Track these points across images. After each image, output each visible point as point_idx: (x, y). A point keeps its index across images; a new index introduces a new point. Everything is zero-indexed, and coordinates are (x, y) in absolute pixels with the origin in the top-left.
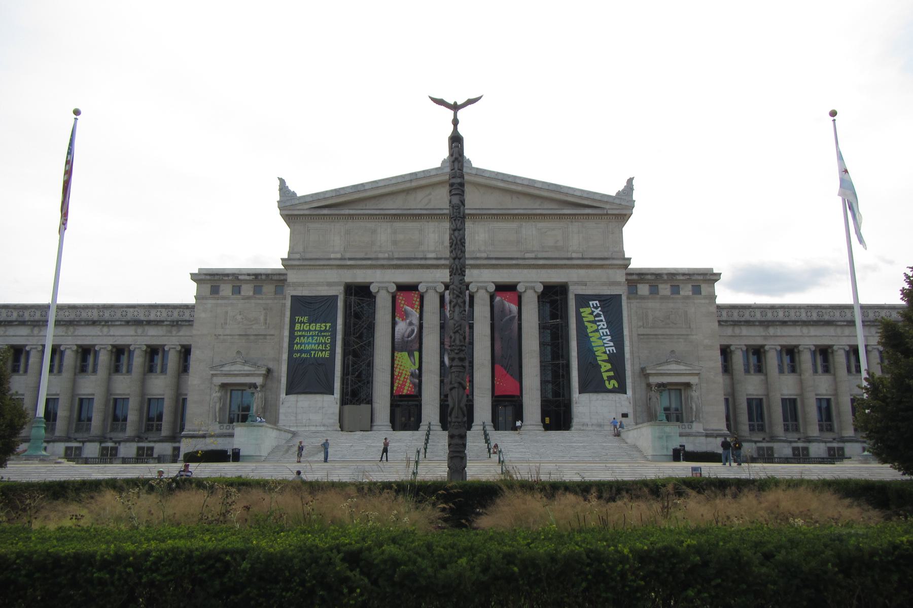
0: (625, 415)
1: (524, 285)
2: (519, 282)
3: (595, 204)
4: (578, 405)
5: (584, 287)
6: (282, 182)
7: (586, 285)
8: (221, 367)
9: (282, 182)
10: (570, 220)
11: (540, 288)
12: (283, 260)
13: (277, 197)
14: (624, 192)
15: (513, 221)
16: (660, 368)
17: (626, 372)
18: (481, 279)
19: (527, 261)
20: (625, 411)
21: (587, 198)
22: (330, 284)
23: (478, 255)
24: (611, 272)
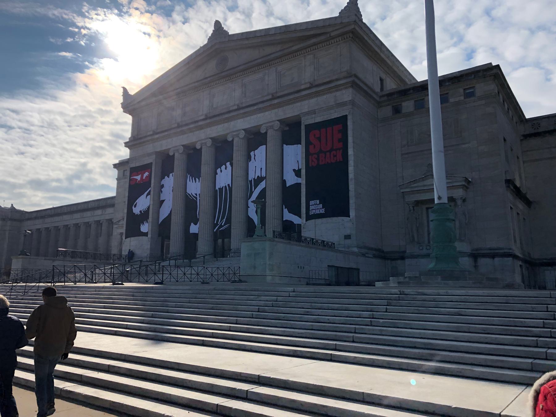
0: (348, 237)
1: (265, 126)
2: (262, 125)
3: (319, 32)
4: (305, 230)
5: (314, 115)
6: (124, 89)
7: (315, 114)
8: (119, 222)
9: (124, 89)
10: (303, 55)
11: (277, 125)
12: (126, 143)
13: (121, 100)
14: (346, 9)
15: (259, 72)
16: (416, 185)
17: (350, 192)
18: (235, 129)
19: (265, 103)
20: (348, 232)
21: (312, 29)
22: (149, 155)
23: (231, 109)
24: (338, 94)
